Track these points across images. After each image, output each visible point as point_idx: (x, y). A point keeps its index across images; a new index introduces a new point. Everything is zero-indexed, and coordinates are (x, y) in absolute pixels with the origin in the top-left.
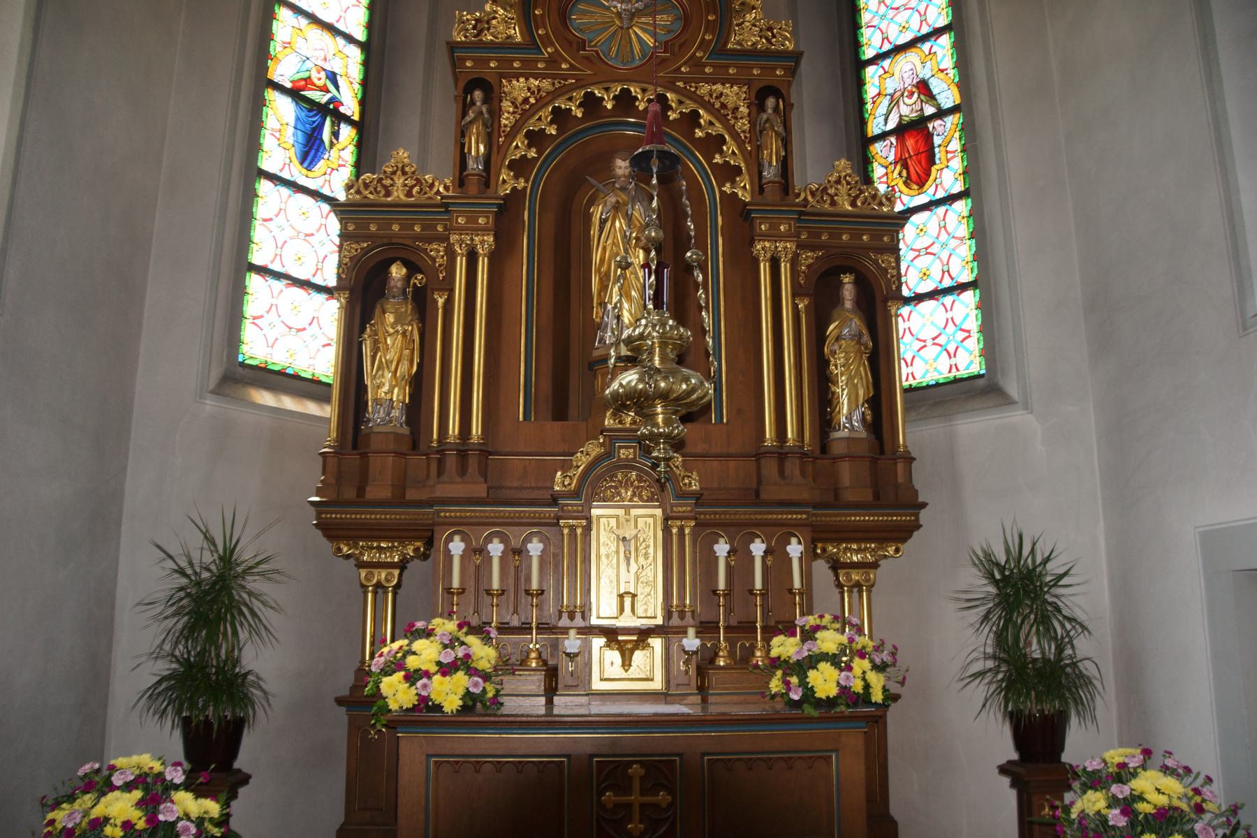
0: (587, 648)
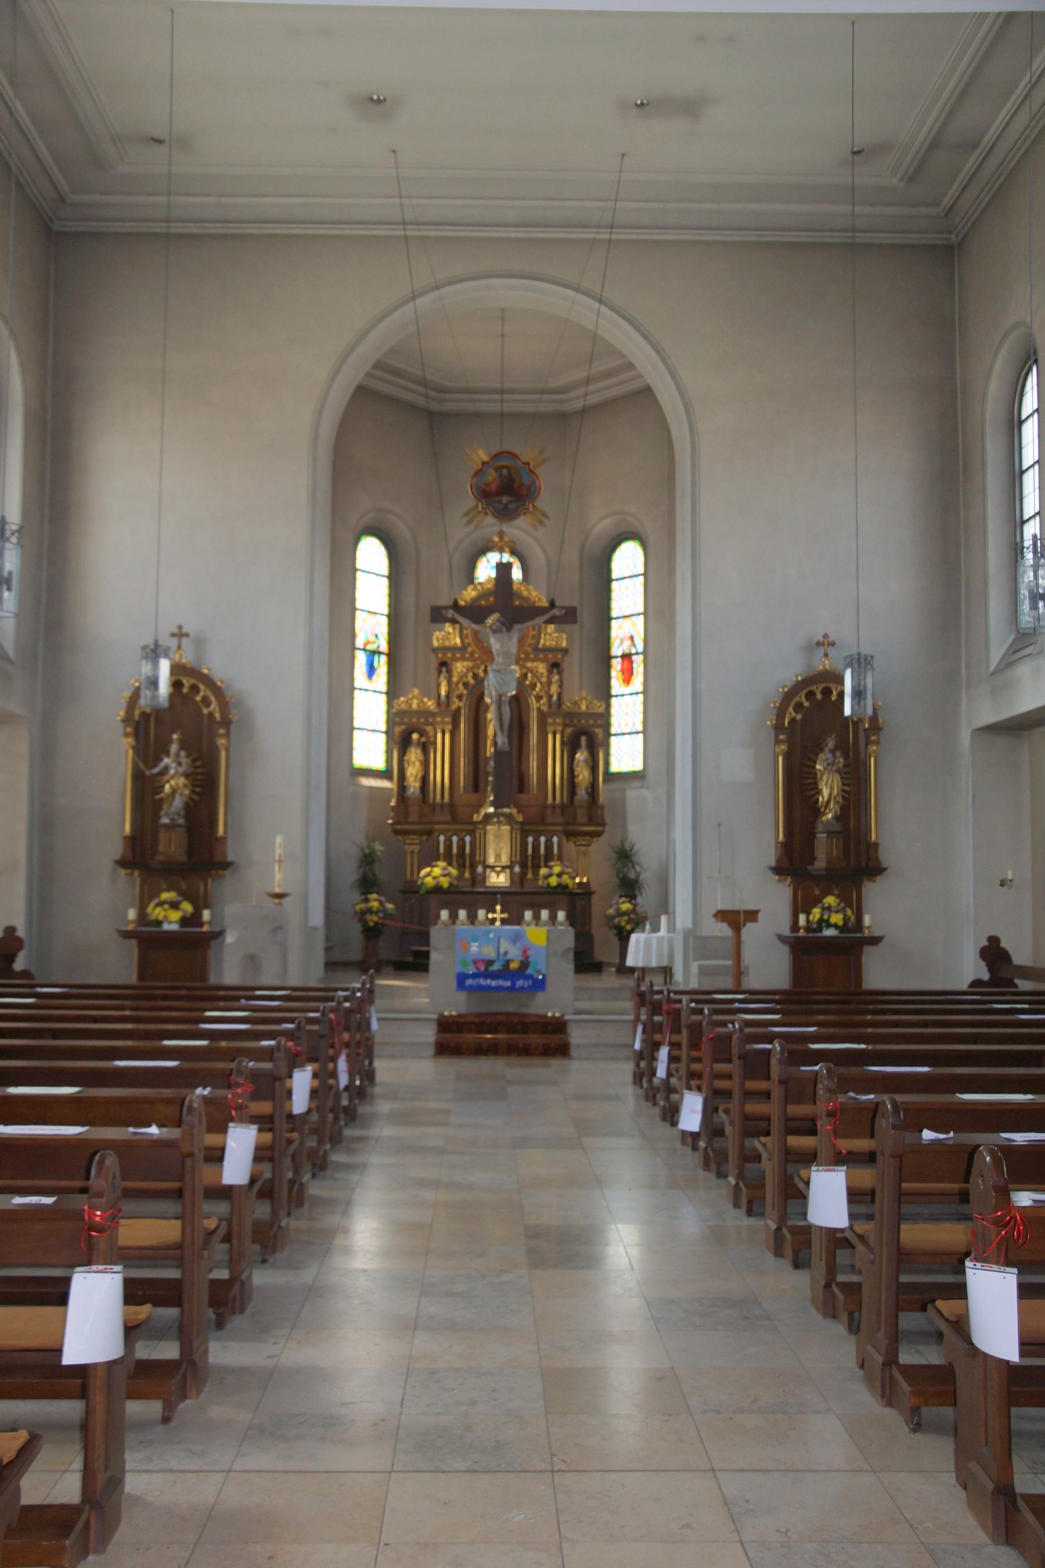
0: (484, 871)
